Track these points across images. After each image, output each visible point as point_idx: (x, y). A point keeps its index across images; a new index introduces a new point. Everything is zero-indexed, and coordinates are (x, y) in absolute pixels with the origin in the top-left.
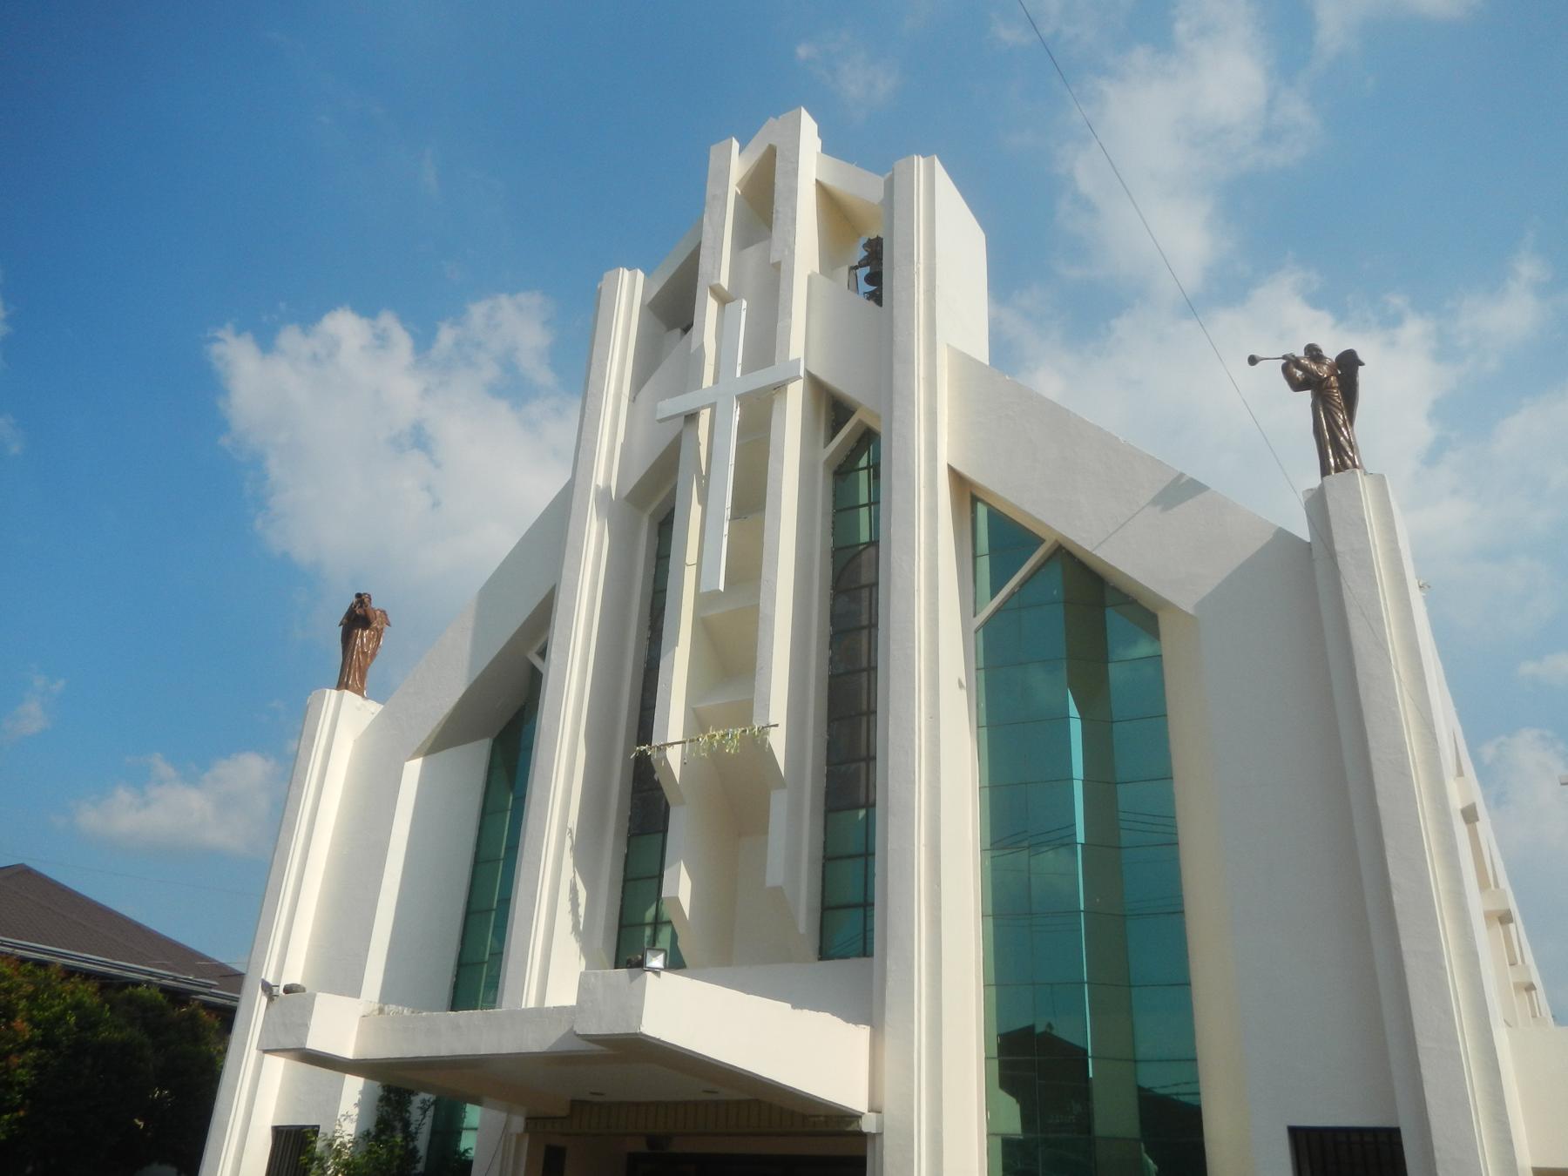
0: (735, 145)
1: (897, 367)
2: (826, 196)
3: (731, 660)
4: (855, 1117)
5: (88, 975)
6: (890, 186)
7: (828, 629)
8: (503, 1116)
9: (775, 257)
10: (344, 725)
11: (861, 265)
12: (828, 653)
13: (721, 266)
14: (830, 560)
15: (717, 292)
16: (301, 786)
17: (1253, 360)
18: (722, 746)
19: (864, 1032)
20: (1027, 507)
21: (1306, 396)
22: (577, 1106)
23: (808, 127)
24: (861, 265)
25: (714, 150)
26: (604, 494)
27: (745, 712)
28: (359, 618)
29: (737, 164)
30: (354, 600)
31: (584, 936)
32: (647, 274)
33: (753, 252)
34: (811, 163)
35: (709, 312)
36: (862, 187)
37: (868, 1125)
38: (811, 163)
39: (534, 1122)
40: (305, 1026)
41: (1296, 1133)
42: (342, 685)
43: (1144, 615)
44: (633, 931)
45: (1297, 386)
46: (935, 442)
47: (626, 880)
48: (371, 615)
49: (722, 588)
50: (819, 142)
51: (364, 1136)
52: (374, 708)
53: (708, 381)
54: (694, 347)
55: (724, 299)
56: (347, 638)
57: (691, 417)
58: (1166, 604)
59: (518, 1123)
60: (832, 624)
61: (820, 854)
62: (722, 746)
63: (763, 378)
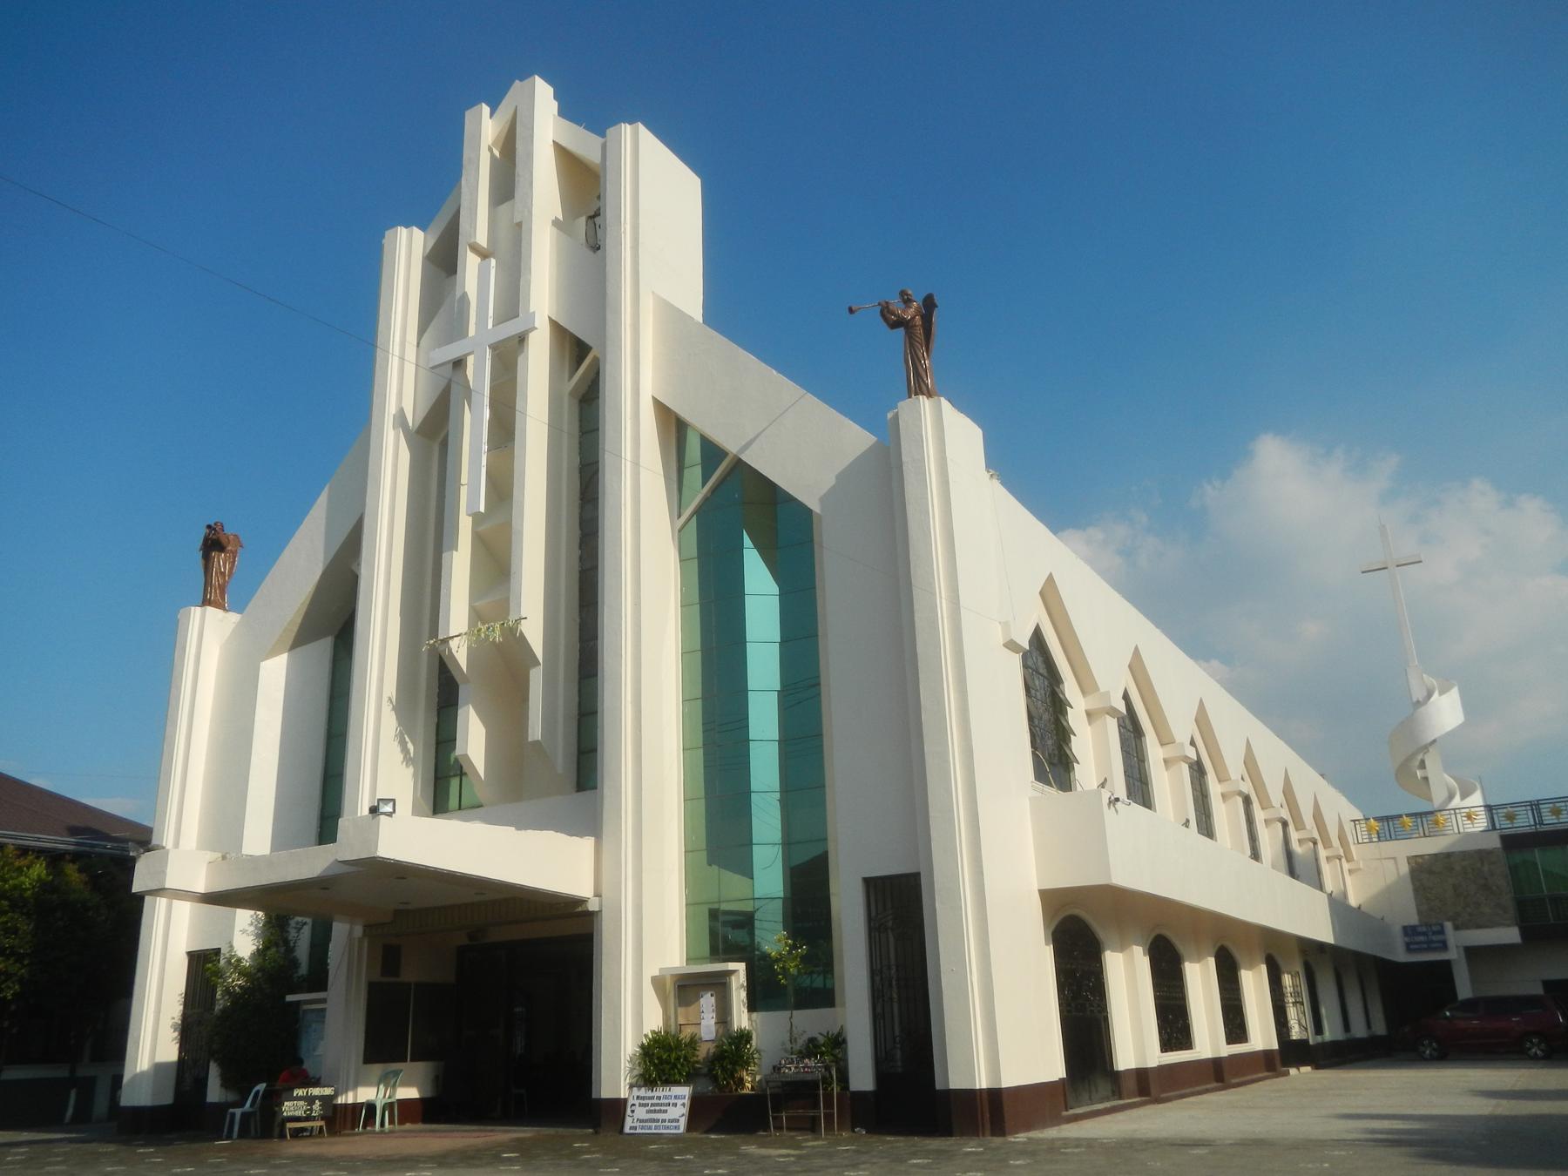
0: (486, 109)
2: (562, 153)
3: (496, 564)
4: (582, 901)
5: (40, 852)
6: (604, 147)
7: (578, 532)
8: (347, 926)
10: (209, 635)
12: (578, 552)
13: (479, 226)
14: (577, 475)
15: (475, 249)
19: (589, 842)
21: (901, 331)
22: (397, 913)
23: (543, 95)
25: (469, 115)
30: (204, 531)
32: (423, 228)
33: (504, 207)
35: (470, 264)
37: (593, 906)
39: (368, 928)
40: (164, 873)
41: (869, 882)
42: (206, 602)
44: (443, 786)
45: (894, 325)
46: (640, 380)
47: (438, 743)
48: (224, 540)
49: (482, 509)
50: (555, 104)
51: (259, 954)
52: (233, 618)
53: (472, 331)
54: (458, 294)
55: (484, 255)
56: (207, 558)
57: (459, 364)
59: (358, 931)
60: (581, 529)
61: (575, 711)
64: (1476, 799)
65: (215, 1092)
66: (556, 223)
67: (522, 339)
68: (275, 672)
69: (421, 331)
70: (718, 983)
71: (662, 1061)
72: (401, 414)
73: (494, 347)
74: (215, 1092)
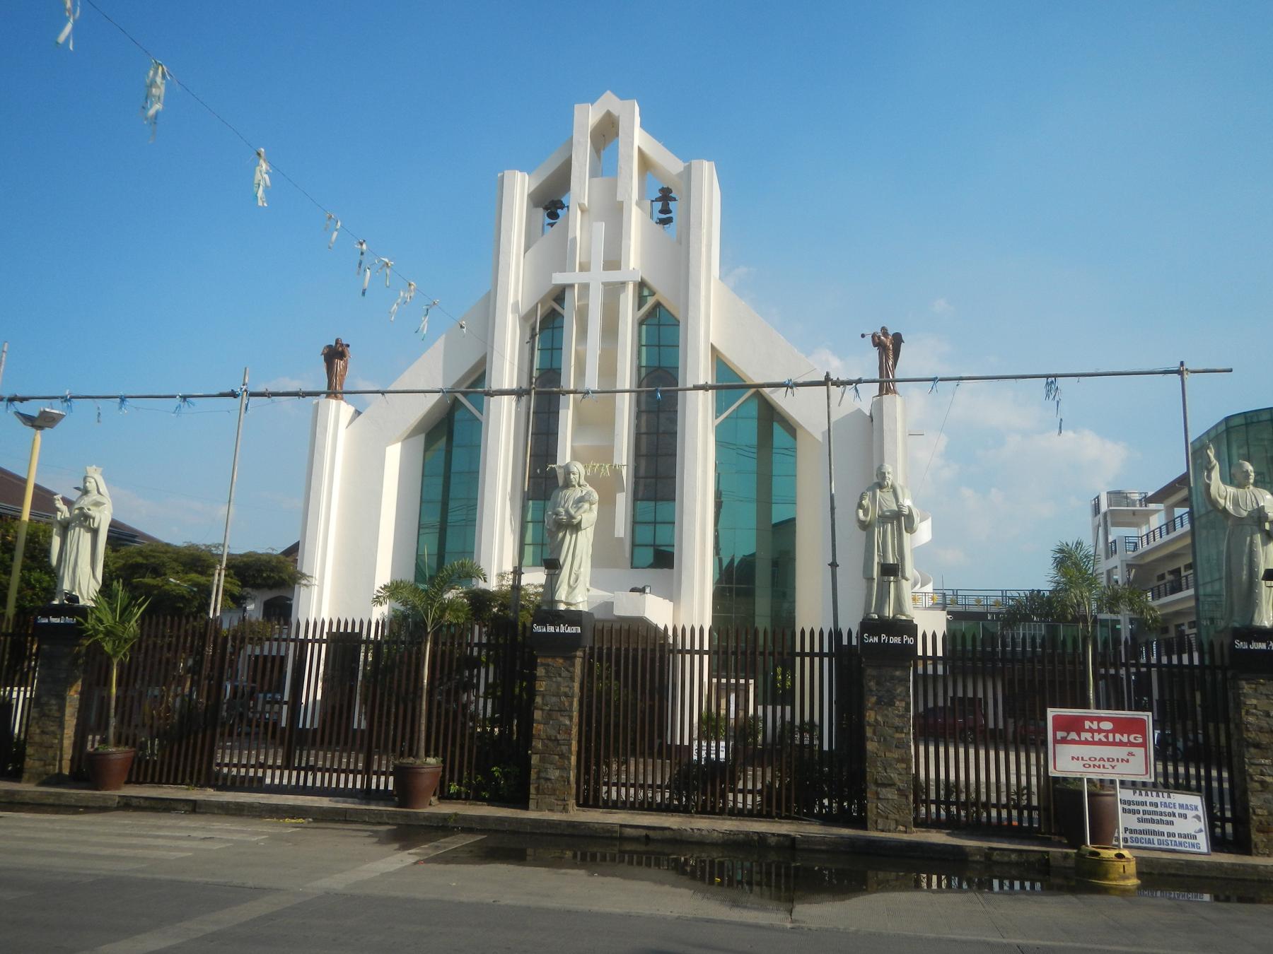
1: (691, 288)
9: (619, 198)
11: (656, 200)
16: (322, 456)
17: (863, 336)
24: (656, 200)
27: (606, 453)
29: (588, 116)
34: (637, 138)
36: (670, 164)
38: (637, 138)
43: (791, 428)
54: (570, 236)
55: (582, 211)
63: (614, 276)
64: (929, 588)
65: (359, 721)
66: (638, 204)
67: (624, 284)
68: (394, 454)
70: (742, 692)
71: (710, 726)
72: (516, 304)
74: (359, 721)
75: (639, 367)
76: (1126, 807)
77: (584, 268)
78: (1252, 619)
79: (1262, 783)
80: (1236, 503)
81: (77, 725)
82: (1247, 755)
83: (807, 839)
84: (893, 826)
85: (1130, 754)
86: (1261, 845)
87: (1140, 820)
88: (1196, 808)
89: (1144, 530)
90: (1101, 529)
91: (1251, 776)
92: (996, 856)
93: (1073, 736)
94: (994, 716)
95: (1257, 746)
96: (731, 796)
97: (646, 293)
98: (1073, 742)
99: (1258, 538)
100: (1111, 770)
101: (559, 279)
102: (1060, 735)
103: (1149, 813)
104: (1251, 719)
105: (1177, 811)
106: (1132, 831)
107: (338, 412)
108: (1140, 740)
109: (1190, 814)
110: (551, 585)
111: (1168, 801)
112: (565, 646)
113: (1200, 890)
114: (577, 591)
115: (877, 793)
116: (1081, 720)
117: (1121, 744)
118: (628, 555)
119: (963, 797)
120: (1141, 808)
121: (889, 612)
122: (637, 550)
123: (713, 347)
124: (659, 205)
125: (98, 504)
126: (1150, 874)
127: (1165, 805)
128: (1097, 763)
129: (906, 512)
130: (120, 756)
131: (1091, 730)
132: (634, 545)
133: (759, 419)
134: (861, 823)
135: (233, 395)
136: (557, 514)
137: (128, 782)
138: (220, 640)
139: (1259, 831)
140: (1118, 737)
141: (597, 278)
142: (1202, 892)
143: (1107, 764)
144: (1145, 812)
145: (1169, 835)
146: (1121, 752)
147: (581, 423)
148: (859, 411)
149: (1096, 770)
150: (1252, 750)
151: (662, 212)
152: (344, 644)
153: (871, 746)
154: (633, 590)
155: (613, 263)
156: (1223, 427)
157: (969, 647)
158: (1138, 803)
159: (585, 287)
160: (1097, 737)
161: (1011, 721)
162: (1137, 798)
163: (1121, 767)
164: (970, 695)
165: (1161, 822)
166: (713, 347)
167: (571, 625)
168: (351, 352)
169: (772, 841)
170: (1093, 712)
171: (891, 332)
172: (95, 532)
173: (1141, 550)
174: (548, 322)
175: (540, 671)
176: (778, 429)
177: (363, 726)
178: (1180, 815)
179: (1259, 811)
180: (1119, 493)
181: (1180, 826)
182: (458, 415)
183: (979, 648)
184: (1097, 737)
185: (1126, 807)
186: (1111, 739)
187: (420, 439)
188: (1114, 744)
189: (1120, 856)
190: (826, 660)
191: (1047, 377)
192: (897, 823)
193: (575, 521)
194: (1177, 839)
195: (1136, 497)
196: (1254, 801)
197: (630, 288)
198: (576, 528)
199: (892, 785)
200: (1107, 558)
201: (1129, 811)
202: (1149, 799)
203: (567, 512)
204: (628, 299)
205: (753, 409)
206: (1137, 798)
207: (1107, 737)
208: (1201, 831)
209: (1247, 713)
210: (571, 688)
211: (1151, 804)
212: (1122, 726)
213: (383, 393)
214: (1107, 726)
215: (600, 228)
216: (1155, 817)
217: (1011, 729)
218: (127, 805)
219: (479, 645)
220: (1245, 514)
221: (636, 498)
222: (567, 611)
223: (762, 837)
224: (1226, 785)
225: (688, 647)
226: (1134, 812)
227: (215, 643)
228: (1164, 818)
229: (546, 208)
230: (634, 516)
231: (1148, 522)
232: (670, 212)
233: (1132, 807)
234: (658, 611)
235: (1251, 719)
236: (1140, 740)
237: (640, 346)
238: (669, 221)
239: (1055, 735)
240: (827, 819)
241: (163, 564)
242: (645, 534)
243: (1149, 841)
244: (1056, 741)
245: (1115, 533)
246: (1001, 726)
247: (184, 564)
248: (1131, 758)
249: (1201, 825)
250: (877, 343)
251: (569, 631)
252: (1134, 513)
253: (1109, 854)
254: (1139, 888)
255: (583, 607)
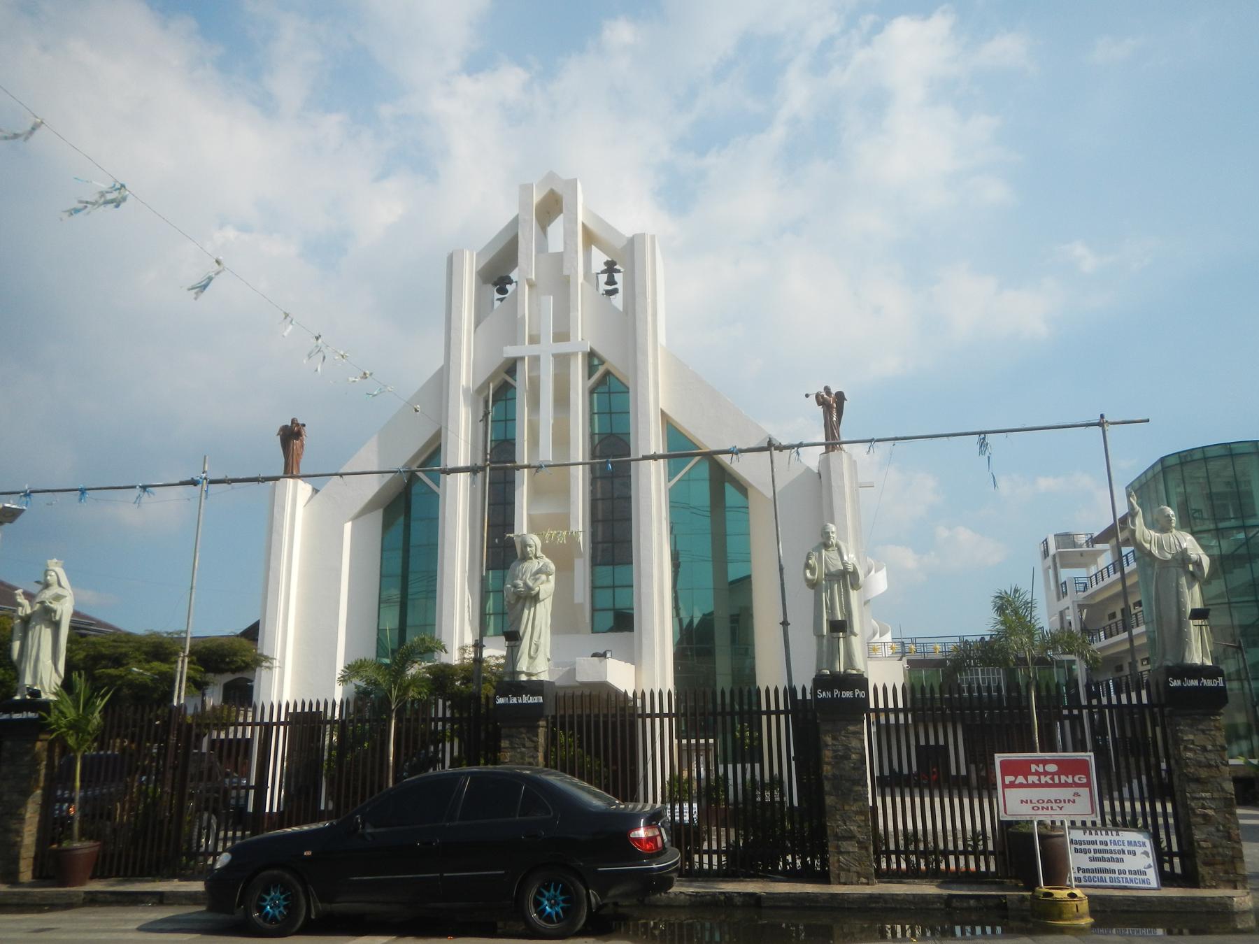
1: (639, 355)
9: (566, 272)
11: (603, 272)
16: (281, 535)
17: (807, 396)
18: (556, 539)
20: (701, 438)
24: (603, 272)
26: (466, 390)
27: (563, 521)
28: (291, 435)
31: (471, 622)
43: (742, 488)
46: (657, 399)
55: (531, 285)
58: (751, 486)
62: (556, 539)
63: (563, 348)
64: (888, 638)
69: (477, 324)
71: (677, 790)
73: (556, 356)
75: (592, 435)
76: (1078, 847)
77: (534, 340)
78: (1183, 657)
79: (1205, 816)
80: (1160, 547)
81: (40, 821)
82: (1188, 790)
83: (772, 896)
84: (855, 879)
85: (1076, 794)
86: (1207, 877)
87: (1092, 859)
88: (1144, 844)
89: (1093, 570)
90: (1051, 572)
91: (1193, 810)
92: (955, 903)
93: (1021, 779)
94: (958, 762)
95: (1198, 780)
96: (696, 857)
97: (596, 362)
98: (1021, 786)
99: (1183, 581)
100: (1059, 812)
101: (511, 352)
102: (1008, 779)
103: (1100, 851)
104: (1189, 754)
105: (1126, 848)
106: (1085, 871)
107: (297, 493)
108: (1085, 781)
109: (1139, 850)
110: (512, 657)
111: (1117, 838)
112: (529, 717)
113: (1153, 925)
114: (537, 661)
115: (838, 847)
116: (1028, 763)
117: (1066, 785)
118: (588, 620)
119: (922, 847)
120: (1092, 847)
121: (840, 667)
122: (596, 614)
123: (663, 412)
124: (604, 278)
125: (58, 598)
126: (1104, 911)
127: (1115, 843)
128: (1045, 805)
129: (851, 569)
130: (86, 851)
131: (1037, 773)
132: (594, 610)
133: (711, 480)
134: (824, 878)
135: (194, 483)
136: (515, 586)
137: (93, 877)
138: (184, 728)
139: (1206, 864)
140: (1063, 778)
141: (547, 349)
142: (1155, 928)
143: (1054, 805)
144: (1095, 851)
145: (1120, 872)
146: (1066, 793)
147: (536, 493)
148: (808, 469)
149: (1045, 812)
150: (1193, 786)
151: (607, 283)
152: (305, 723)
153: (829, 800)
154: (594, 655)
155: (562, 335)
156: (1159, 467)
157: (928, 696)
158: (1089, 843)
159: (535, 360)
160: (1043, 780)
161: (973, 767)
162: (1087, 837)
163: (1069, 808)
164: (932, 742)
165: (1112, 860)
166: (663, 412)
167: (533, 695)
168: (307, 432)
169: (738, 901)
170: (1039, 755)
171: (834, 391)
172: (56, 626)
173: (1090, 591)
174: (500, 392)
175: (505, 744)
176: (730, 490)
177: (331, 806)
178: (1129, 852)
179: (1203, 844)
180: (1067, 535)
181: (1130, 863)
182: (416, 489)
183: (937, 695)
184: (1043, 780)
185: (1078, 847)
186: (1057, 781)
187: (377, 517)
188: (1060, 785)
189: (1072, 896)
190: (782, 717)
191: (979, 433)
192: (859, 875)
193: (533, 592)
194: (1127, 875)
195: (1082, 539)
196: (1198, 835)
197: (580, 357)
198: (535, 599)
199: (850, 837)
200: (1059, 599)
201: (1081, 851)
202: (1099, 838)
203: (525, 584)
204: (578, 370)
205: (704, 471)
206: (1087, 837)
207: (1053, 779)
208: (1149, 866)
209: (1186, 749)
210: (535, 757)
211: (1101, 843)
212: (1067, 767)
213: (341, 475)
214: (1052, 768)
215: (549, 302)
216: (1106, 856)
217: (974, 776)
218: (93, 900)
219: (444, 719)
220: (1169, 556)
221: (595, 562)
222: (529, 682)
223: (729, 897)
224: (1171, 821)
225: (648, 711)
226: (1086, 851)
227: (179, 730)
228: (1114, 856)
229: (495, 284)
230: (593, 581)
231: (1095, 562)
232: (615, 283)
233: (1083, 847)
234: (621, 676)
235: (1189, 754)
236: (1085, 781)
237: (592, 414)
238: (615, 291)
239: (1003, 780)
240: (792, 876)
241: (126, 655)
242: (605, 599)
243: (1102, 880)
244: (1005, 786)
245: (1066, 574)
246: (963, 772)
247: (146, 653)
248: (1077, 799)
249: (1150, 860)
250: (821, 401)
251: (531, 701)
252: (1082, 554)
253: (1061, 894)
254: (1093, 926)
255: (544, 677)
